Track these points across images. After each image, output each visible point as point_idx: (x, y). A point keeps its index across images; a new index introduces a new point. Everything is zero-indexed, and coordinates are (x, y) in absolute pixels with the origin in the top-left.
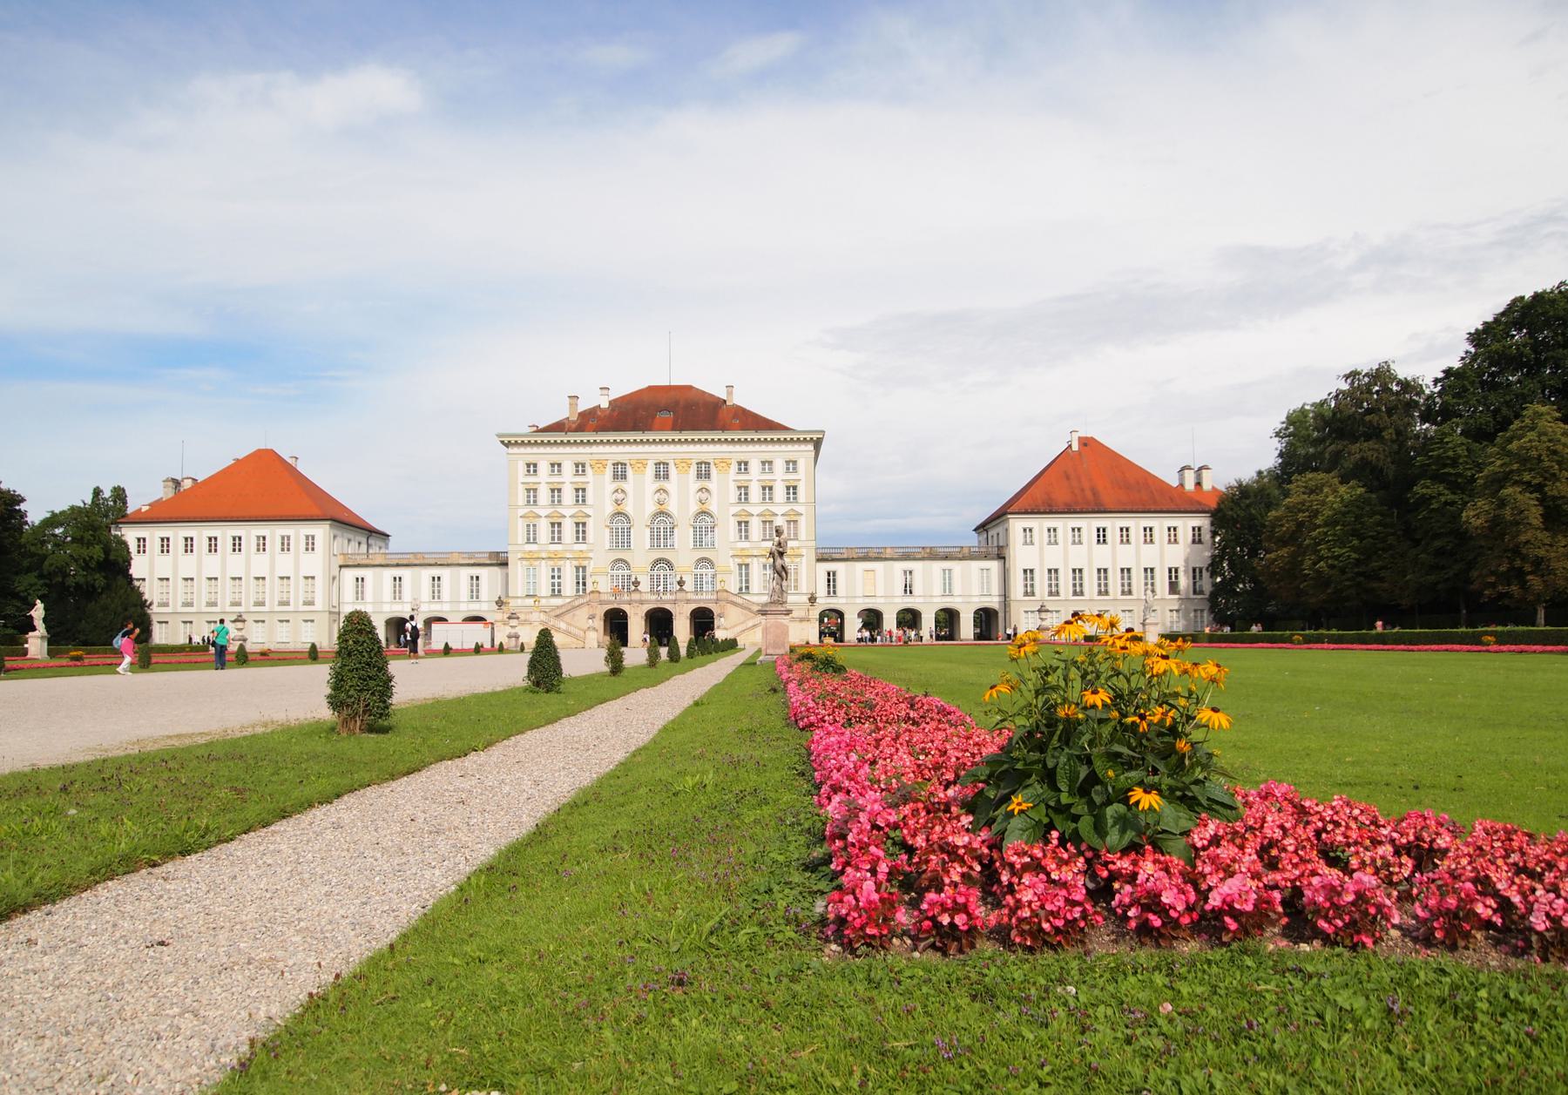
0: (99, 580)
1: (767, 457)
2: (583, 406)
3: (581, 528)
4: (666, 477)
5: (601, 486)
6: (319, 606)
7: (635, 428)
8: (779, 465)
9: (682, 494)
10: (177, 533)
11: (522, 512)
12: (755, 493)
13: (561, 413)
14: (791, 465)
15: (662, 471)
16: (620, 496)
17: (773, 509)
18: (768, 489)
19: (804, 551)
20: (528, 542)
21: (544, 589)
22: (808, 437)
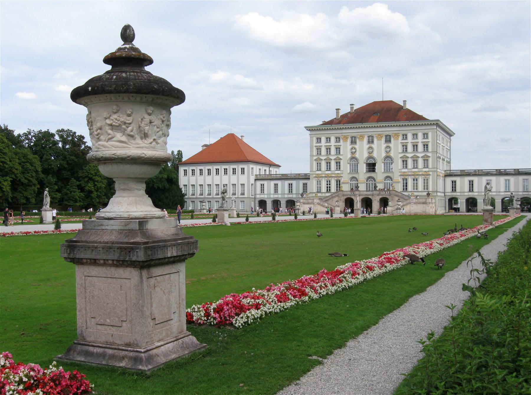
0: (167, 185)
1: (415, 132)
2: (341, 113)
3: (338, 164)
4: (373, 142)
5: (346, 147)
6: (246, 196)
7: (362, 122)
8: (420, 136)
9: (379, 150)
10: (197, 168)
11: (315, 158)
12: (410, 148)
13: (332, 116)
14: (425, 136)
16: (354, 150)
17: (418, 155)
18: (415, 146)
19: (431, 173)
20: (318, 170)
21: (324, 189)
22: (432, 123)
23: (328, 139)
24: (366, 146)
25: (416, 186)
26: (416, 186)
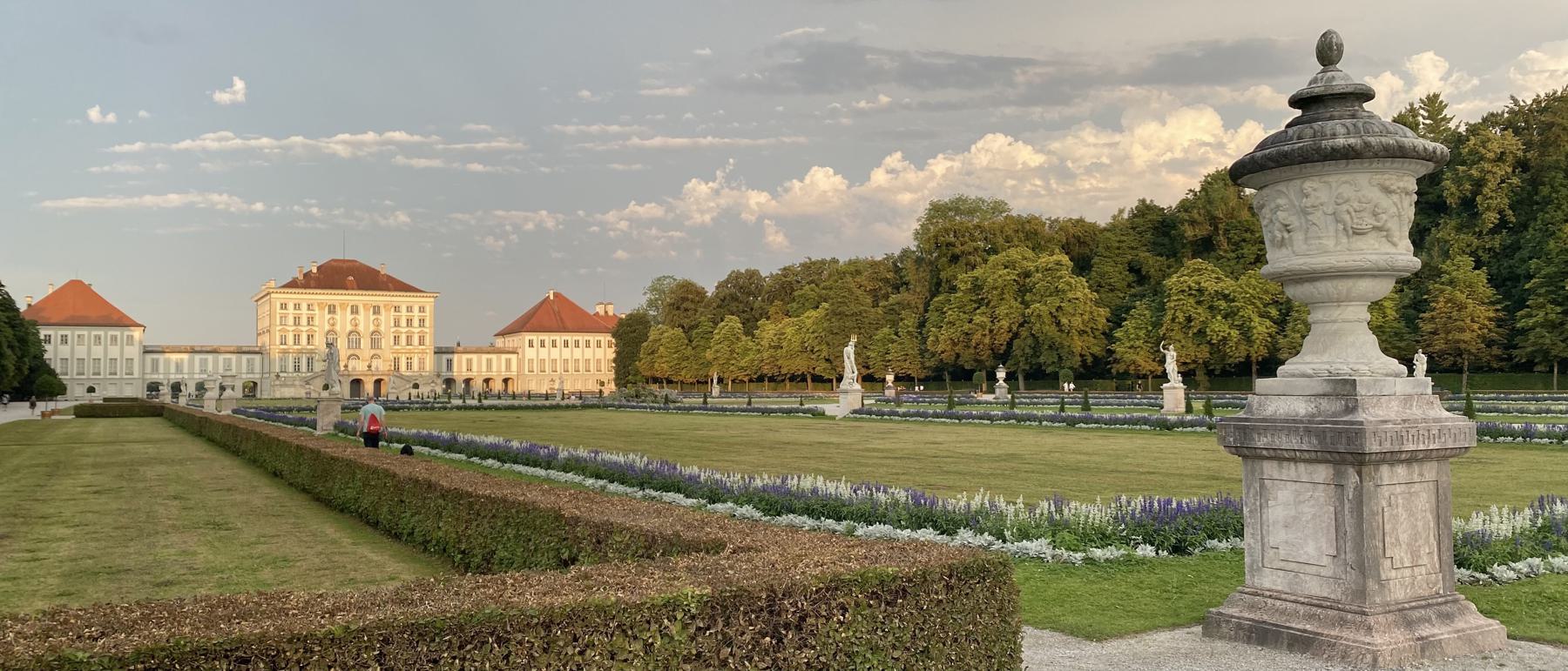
5: (322, 320)
6: (136, 375)
8: (416, 309)
9: (365, 322)
12: (403, 323)
14: (422, 309)
15: (355, 310)
21: (291, 368)
23: (297, 306)
24: (349, 317)
25: (409, 366)
26: (409, 366)
